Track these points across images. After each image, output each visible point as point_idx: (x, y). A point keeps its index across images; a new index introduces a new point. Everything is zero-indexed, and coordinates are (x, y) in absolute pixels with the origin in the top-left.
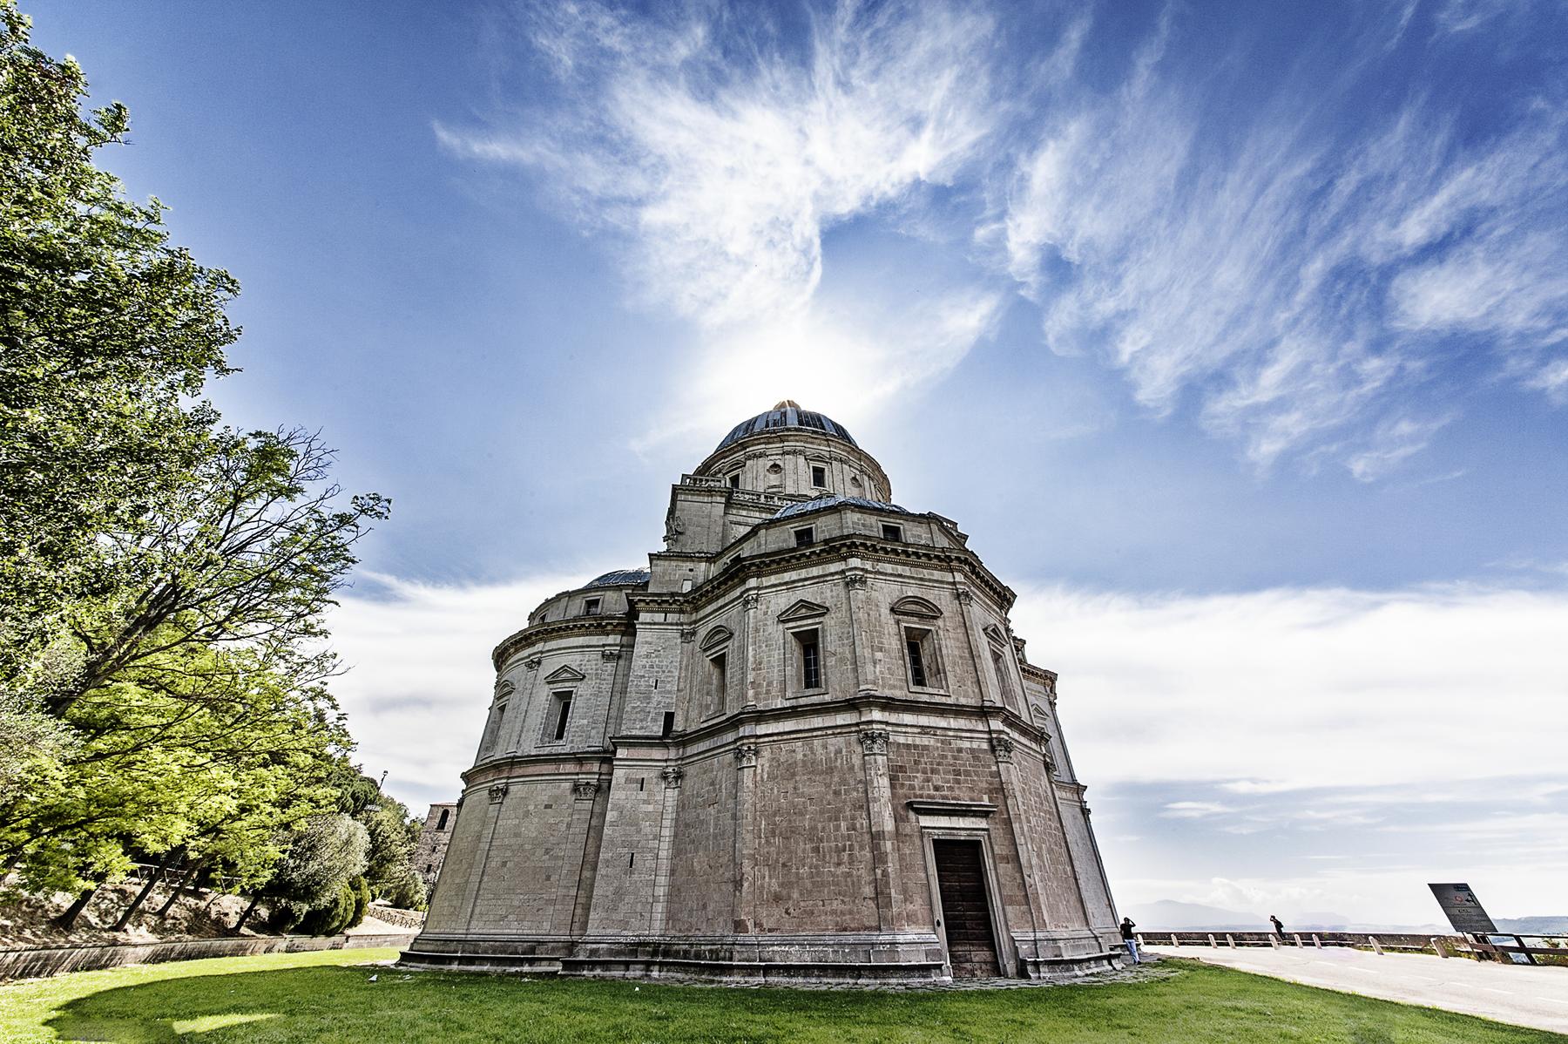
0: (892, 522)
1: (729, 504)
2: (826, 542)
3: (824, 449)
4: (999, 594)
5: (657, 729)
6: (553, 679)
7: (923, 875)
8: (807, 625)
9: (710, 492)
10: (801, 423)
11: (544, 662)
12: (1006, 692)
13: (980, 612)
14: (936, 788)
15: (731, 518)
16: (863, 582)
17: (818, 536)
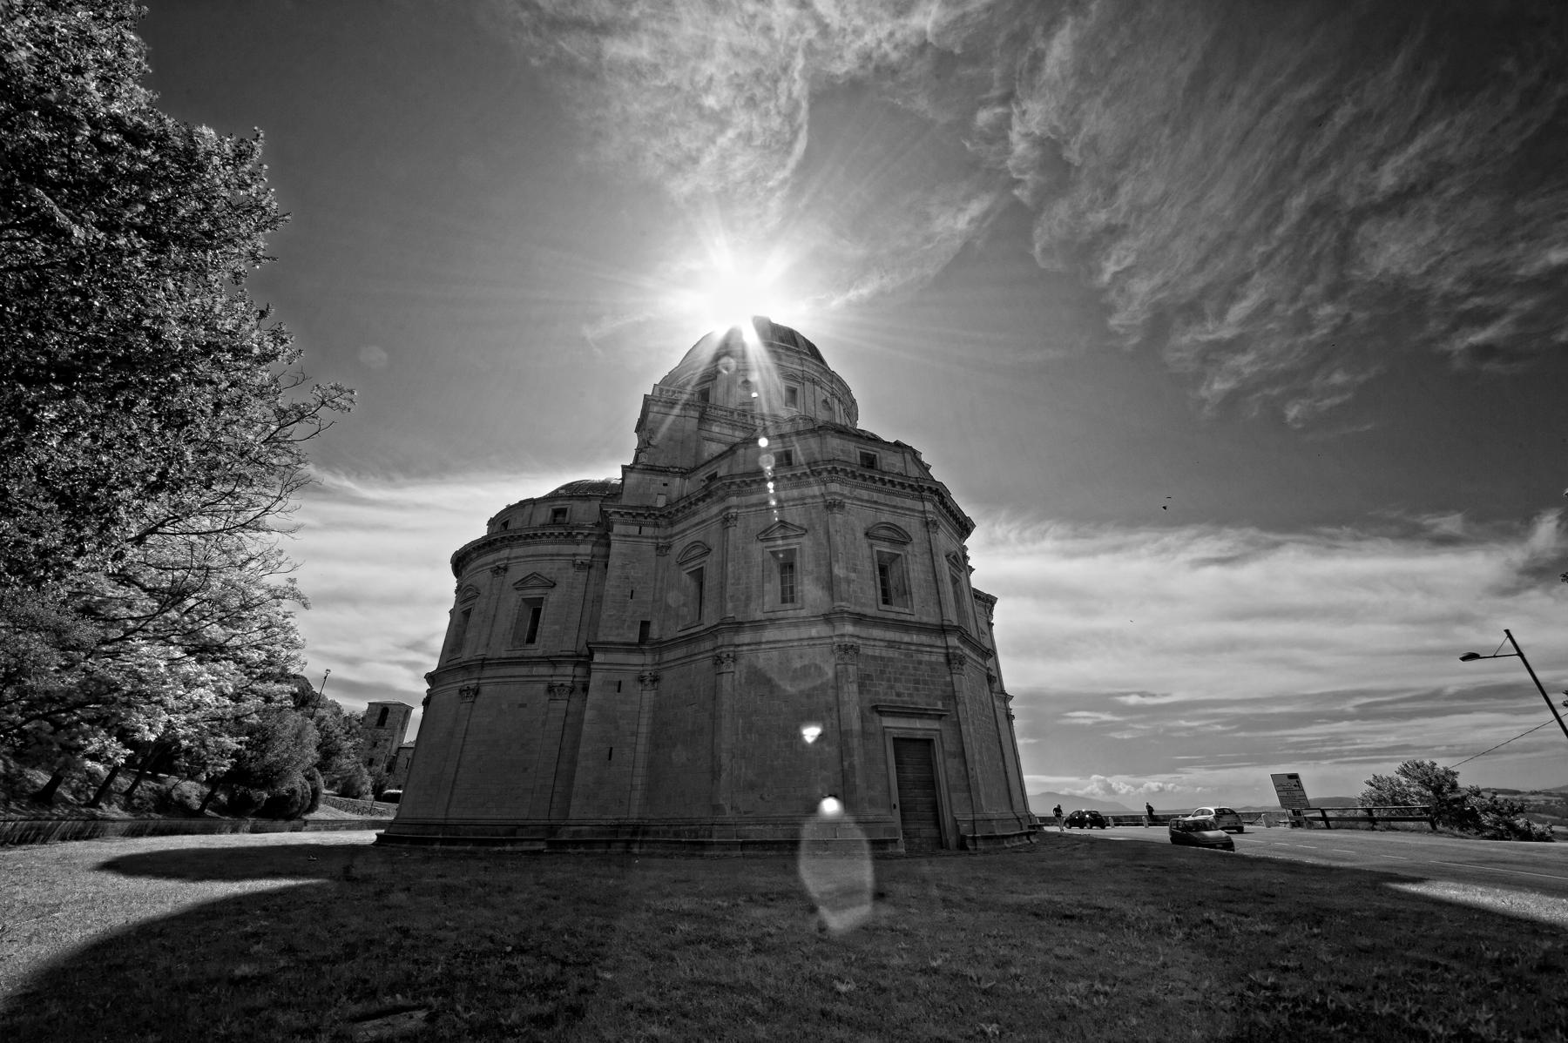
0: (870, 449)
4: (960, 523)
5: (634, 636)
6: (521, 584)
7: (883, 767)
13: (944, 539)
14: (898, 695)
16: (841, 506)
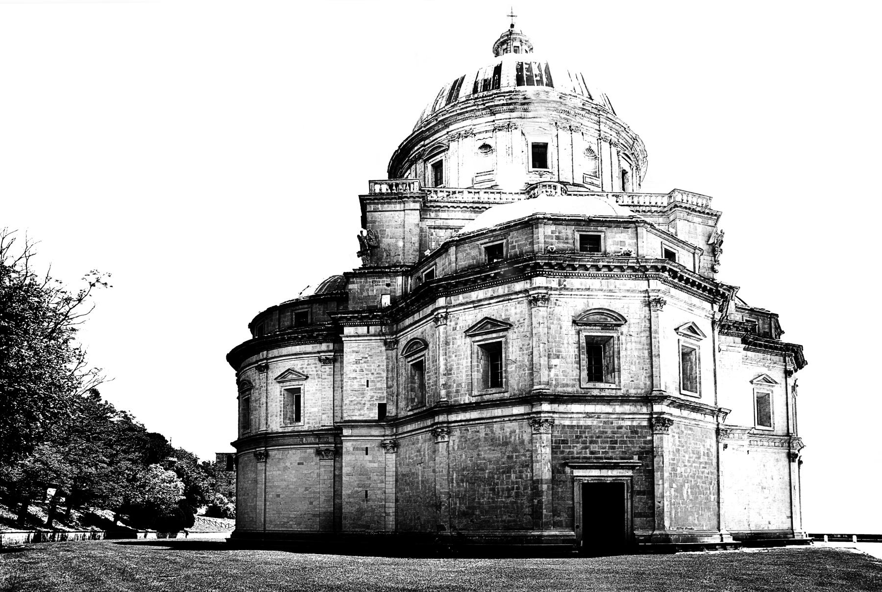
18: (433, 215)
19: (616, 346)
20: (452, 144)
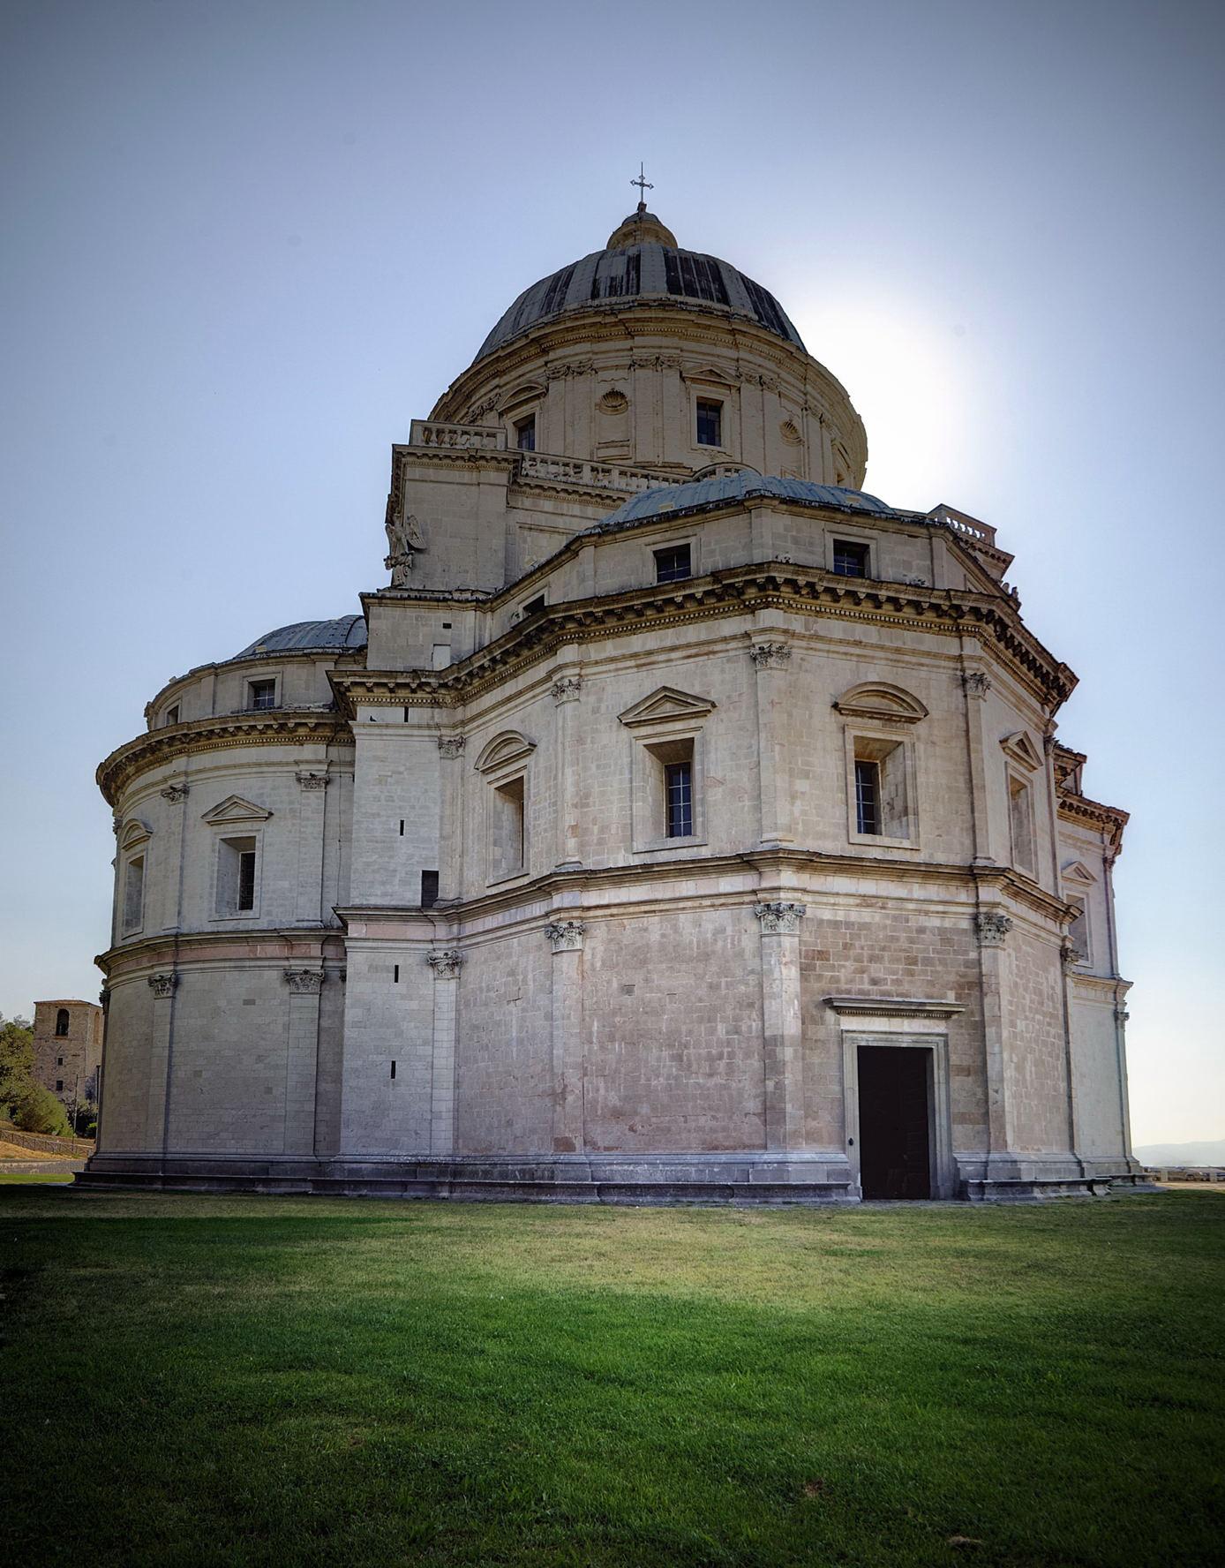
1: (516, 483)
2: (716, 576)
3: (722, 354)
4: (1045, 677)
5: (414, 896)
6: (217, 816)
7: (837, 1088)
8: (674, 731)
9: (474, 459)
10: (673, 287)
11: (193, 790)
12: (1021, 845)
13: (1002, 710)
15: (520, 516)
16: (783, 653)
17: (701, 562)
18: (528, 503)
19: (909, 762)
20: (553, 386)
